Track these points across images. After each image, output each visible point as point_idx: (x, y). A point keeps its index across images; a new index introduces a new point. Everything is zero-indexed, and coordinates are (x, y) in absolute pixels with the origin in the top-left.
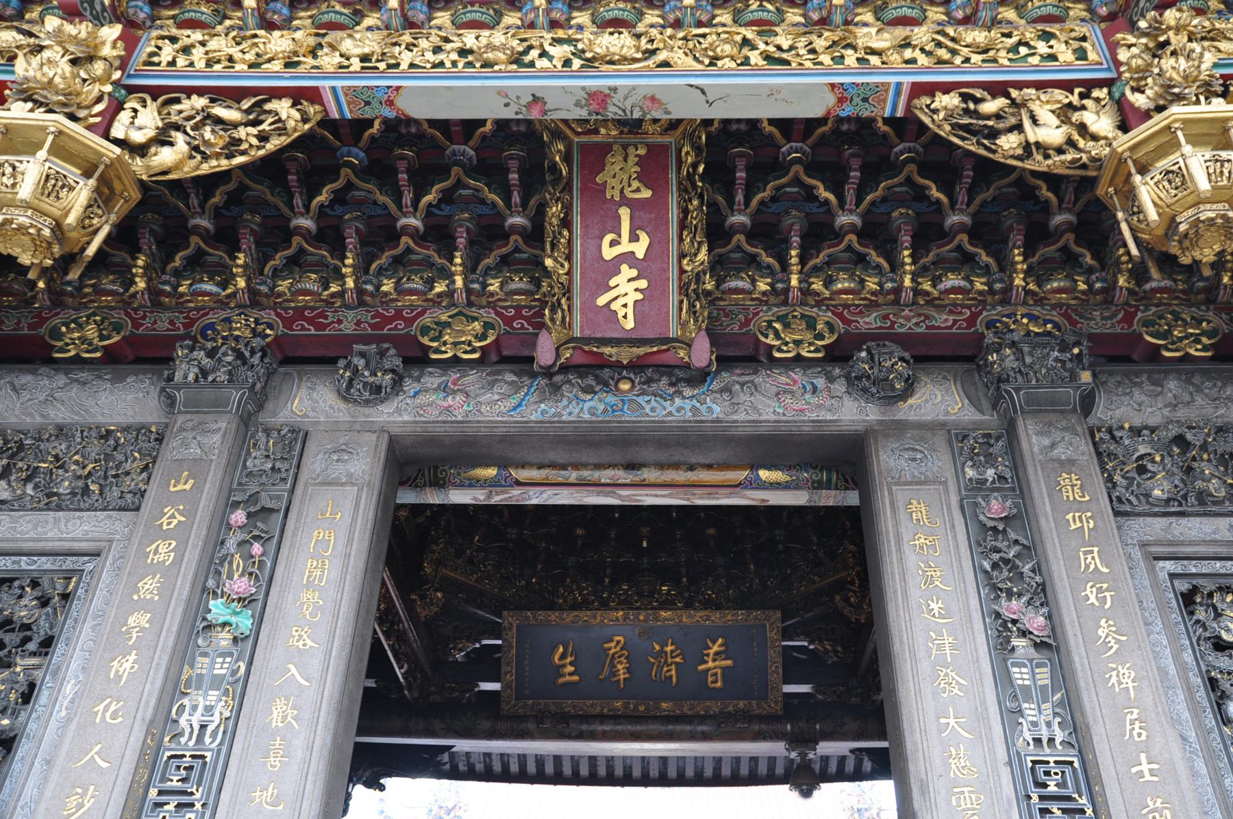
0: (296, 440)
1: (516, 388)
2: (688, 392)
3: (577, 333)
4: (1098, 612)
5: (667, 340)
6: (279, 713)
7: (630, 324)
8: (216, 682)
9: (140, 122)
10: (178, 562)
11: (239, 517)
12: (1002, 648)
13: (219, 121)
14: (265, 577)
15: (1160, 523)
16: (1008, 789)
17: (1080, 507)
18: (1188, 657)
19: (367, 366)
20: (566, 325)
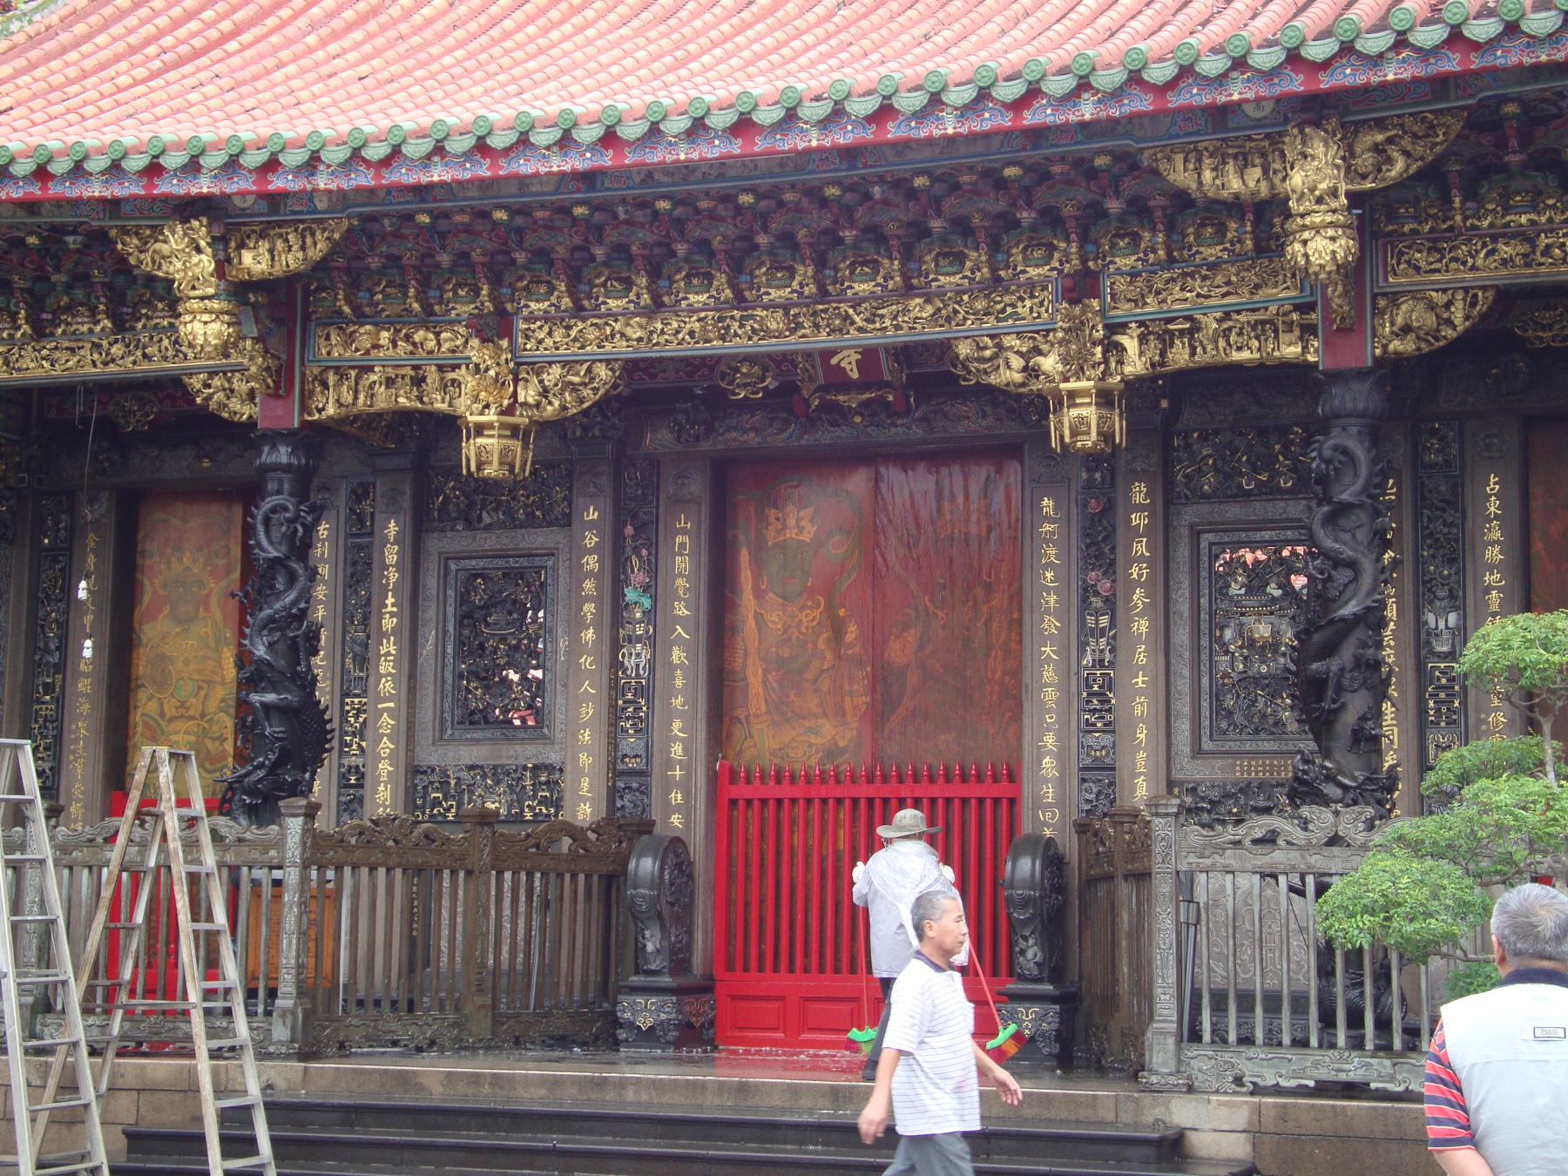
0: (654, 463)
1: (787, 423)
2: (899, 422)
3: (821, 381)
4: (1138, 584)
5: (882, 385)
6: (677, 655)
7: (855, 375)
8: (639, 639)
9: (527, 394)
10: (601, 569)
11: (629, 530)
12: (1085, 602)
13: (571, 383)
14: (652, 569)
15: (1205, 508)
16: (1074, 689)
17: (1140, 508)
18: (1204, 601)
19: (688, 421)
20: (812, 379)
